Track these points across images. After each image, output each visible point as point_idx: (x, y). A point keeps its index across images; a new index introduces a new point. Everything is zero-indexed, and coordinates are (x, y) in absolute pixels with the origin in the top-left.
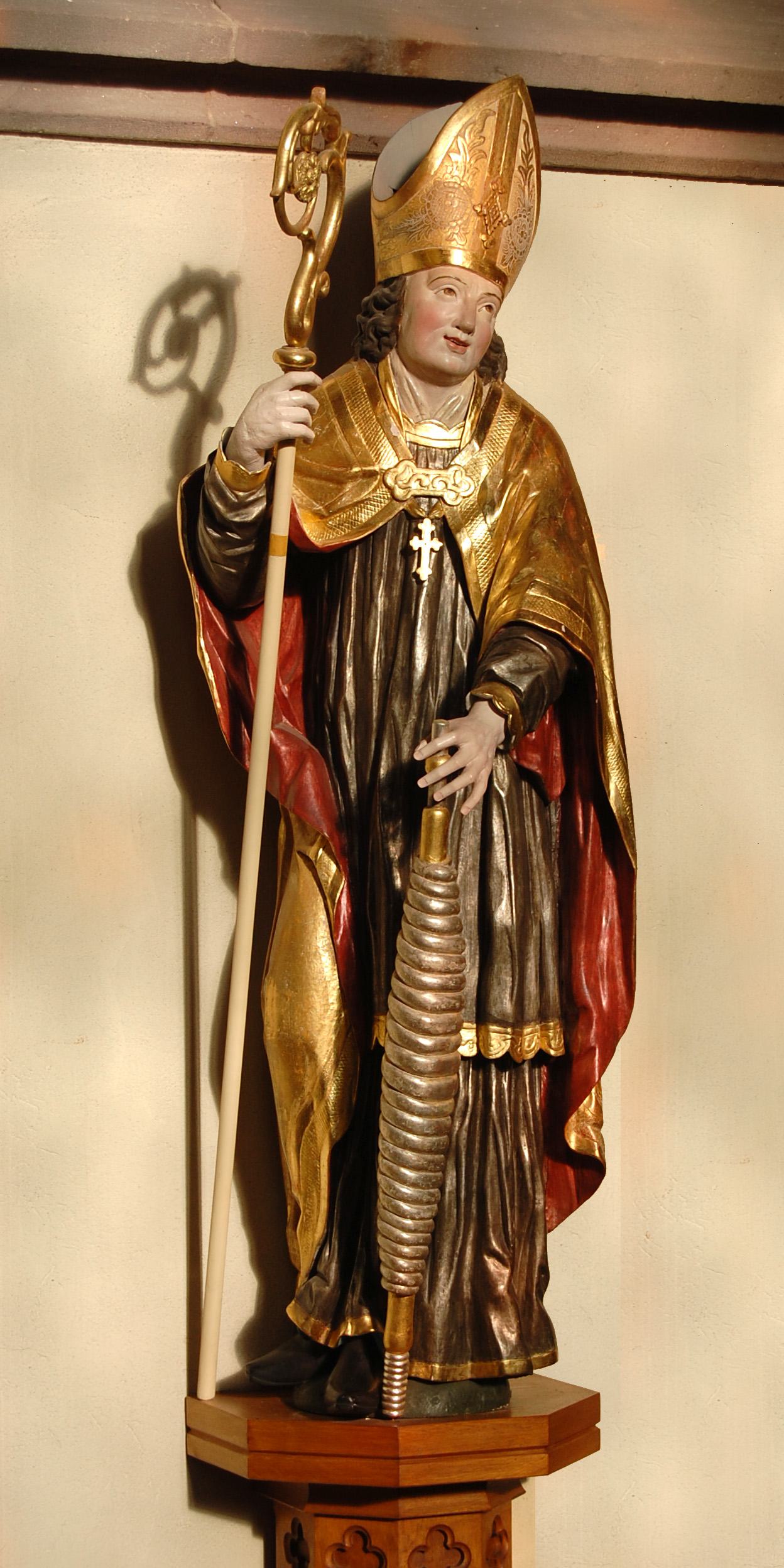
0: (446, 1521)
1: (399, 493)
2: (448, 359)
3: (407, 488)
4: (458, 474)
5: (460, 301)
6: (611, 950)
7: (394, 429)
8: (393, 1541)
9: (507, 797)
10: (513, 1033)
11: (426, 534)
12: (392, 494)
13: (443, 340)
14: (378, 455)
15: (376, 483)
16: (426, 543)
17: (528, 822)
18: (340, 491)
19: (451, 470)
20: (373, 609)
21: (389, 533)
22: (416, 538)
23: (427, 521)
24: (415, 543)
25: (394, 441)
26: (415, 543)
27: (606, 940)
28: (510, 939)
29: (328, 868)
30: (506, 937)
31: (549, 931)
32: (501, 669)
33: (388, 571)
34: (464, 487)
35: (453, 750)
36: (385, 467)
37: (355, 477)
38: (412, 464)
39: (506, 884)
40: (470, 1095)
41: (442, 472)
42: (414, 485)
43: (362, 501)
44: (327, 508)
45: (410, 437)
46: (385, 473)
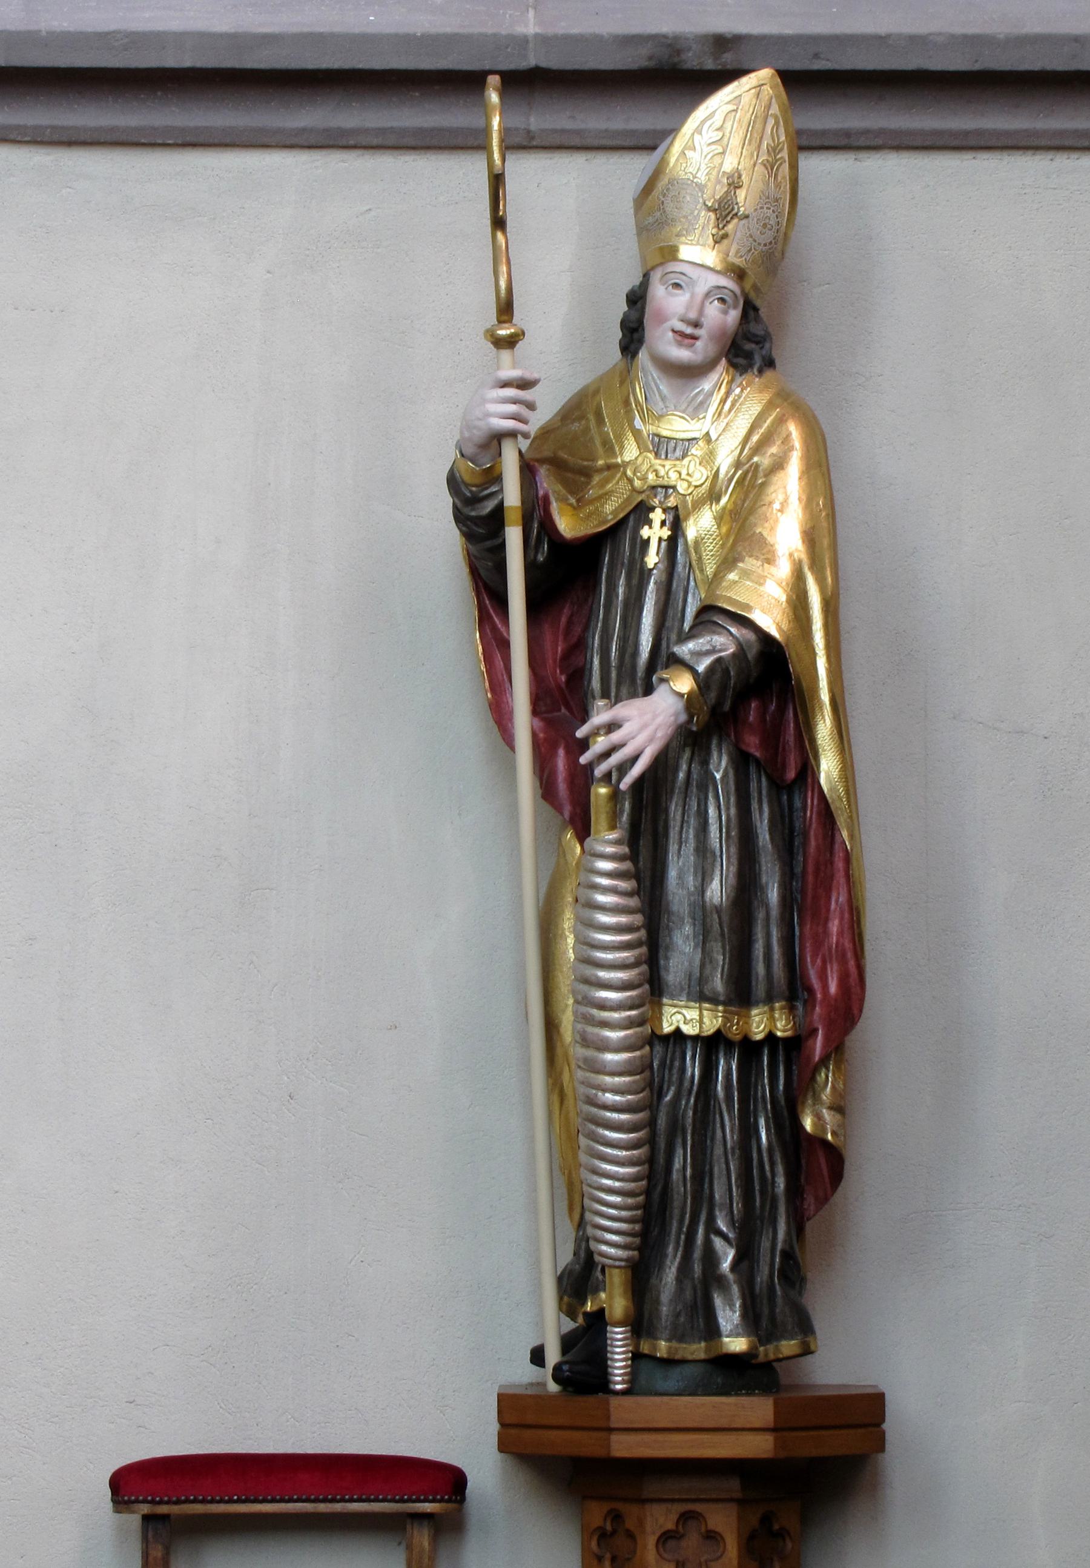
0: (698, 1507)
1: (637, 483)
2: (681, 354)
3: (644, 479)
4: (693, 463)
5: (687, 296)
6: (841, 933)
7: (638, 423)
8: (641, 1523)
9: (722, 778)
10: (724, 1012)
11: (657, 524)
12: (632, 485)
13: (670, 334)
14: (622, 447)
15: (619, 475)
16: (655, 532)
17: (755, 805)
18: (588, 483)
19: (686, 461)
20: (614, 598)
21: (631, 523)
22: (646, 527)
23: (658, 511)
24: (645, 532)
25: (637, 434)
26: (645, 532)
27: (836, 922)
28: (720, 918)
29: (573, 850)
30: (715, 916)
31: (775, 912)
32: (685, 650)
33: (629, 561)
34: (697, 475)
35: (611, 727)
36: (627, 459)
37: (600, 470)
38: (651, 456)
39: (718, 864)
40: (697, 1073)
41: (678, 462)
42: (651, 476)
43: (606, 494)
44: (578, 501)
45: (652, 429)
46: (625, 464)
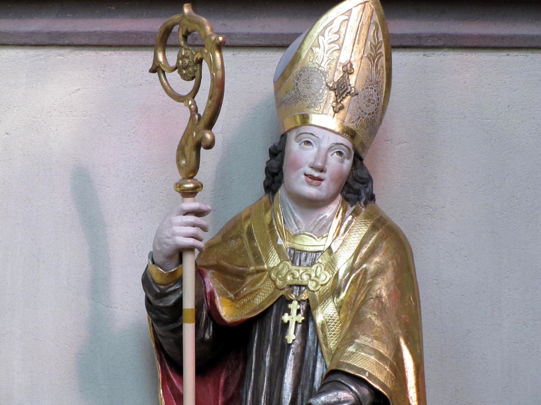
1: (279, 283)
2: (310, 191)
3: (284, 279)
4: (319, 269)
5: (315, 149)
7: (280, 242)
11: (294, 312)
12: (275, 284)
13: (303, 177)
14: (267, 258)
16: (293, 318)
18: (243, 283)
19: (314, 267)
20: (263, 365)
21: (274, 311)
22: (286, 314)
23: (295, 303)
24: (286, 318)
26: (286, 318)
33: (273, 338)
34: (323, 277)
36: (271, 265)
37: (252, 274)
38: (289, 263)
41: (308, 268)
42: (289, 278)
43: (256, 291)
44: (236, 295)
46: (270, 270)
